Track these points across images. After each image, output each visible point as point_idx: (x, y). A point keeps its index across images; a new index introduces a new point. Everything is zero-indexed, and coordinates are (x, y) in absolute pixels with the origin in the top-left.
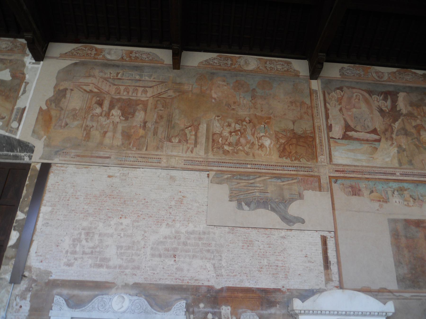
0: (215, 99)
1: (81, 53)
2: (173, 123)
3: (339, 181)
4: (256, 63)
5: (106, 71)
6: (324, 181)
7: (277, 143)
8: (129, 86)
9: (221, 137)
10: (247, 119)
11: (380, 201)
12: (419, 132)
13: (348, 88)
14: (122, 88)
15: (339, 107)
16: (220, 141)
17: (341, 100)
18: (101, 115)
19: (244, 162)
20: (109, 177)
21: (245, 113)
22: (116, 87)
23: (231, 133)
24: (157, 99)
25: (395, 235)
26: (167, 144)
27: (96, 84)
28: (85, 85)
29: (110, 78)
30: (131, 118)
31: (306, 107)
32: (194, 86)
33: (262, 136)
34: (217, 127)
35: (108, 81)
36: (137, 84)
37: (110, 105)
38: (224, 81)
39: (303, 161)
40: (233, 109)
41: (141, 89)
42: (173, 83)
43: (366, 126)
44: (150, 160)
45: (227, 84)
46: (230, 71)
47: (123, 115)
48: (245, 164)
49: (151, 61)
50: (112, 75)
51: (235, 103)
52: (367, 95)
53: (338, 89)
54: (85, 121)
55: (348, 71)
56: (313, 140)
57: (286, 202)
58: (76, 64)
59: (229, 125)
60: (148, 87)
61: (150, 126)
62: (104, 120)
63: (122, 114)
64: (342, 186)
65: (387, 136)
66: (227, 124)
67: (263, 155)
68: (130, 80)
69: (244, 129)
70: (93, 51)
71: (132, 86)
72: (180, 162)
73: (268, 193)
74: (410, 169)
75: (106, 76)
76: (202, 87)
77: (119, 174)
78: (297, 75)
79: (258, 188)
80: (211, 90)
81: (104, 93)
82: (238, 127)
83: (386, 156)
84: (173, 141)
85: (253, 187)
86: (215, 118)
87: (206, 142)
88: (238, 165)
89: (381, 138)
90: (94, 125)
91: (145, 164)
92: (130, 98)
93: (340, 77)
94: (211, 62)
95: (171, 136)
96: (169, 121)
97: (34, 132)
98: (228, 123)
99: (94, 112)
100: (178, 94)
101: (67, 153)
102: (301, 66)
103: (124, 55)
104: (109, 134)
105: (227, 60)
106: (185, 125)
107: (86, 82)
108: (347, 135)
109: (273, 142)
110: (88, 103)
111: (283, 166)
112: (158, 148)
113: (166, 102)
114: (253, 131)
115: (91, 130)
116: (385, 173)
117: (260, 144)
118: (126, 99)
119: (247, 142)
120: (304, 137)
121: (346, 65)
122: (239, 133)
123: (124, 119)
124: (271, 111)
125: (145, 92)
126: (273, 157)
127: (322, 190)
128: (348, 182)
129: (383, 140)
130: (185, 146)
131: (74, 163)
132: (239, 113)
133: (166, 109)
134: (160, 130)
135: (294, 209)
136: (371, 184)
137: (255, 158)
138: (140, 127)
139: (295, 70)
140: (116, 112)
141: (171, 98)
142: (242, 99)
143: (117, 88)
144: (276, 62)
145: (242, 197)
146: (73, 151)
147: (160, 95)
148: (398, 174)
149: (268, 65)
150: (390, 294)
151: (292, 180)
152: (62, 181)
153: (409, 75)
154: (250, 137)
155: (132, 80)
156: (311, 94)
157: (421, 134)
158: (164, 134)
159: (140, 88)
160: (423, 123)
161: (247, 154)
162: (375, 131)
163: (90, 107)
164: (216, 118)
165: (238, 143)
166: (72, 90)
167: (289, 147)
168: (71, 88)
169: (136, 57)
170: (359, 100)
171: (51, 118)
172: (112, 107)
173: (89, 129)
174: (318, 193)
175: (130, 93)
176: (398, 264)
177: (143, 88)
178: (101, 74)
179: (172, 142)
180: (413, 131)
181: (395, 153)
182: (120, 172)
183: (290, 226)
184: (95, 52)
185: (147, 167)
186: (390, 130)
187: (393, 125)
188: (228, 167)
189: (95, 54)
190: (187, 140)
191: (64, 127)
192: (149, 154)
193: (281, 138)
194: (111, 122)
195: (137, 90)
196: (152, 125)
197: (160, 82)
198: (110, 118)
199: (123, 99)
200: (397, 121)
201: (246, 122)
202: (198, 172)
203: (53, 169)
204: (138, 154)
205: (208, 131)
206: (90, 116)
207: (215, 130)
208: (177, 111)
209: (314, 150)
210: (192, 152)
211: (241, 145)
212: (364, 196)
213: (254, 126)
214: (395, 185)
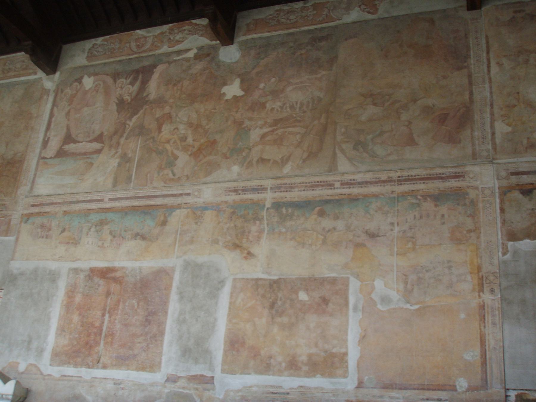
11: (68, 243)
55: (100, 49)
89: (103, 147)
121: (100, 40)
128: (39, 220)
129: (106, 149)
148: (106, 199)
157: (162, 130)
162: (99, 139)
170: (97, 92)
187: (128, 122)
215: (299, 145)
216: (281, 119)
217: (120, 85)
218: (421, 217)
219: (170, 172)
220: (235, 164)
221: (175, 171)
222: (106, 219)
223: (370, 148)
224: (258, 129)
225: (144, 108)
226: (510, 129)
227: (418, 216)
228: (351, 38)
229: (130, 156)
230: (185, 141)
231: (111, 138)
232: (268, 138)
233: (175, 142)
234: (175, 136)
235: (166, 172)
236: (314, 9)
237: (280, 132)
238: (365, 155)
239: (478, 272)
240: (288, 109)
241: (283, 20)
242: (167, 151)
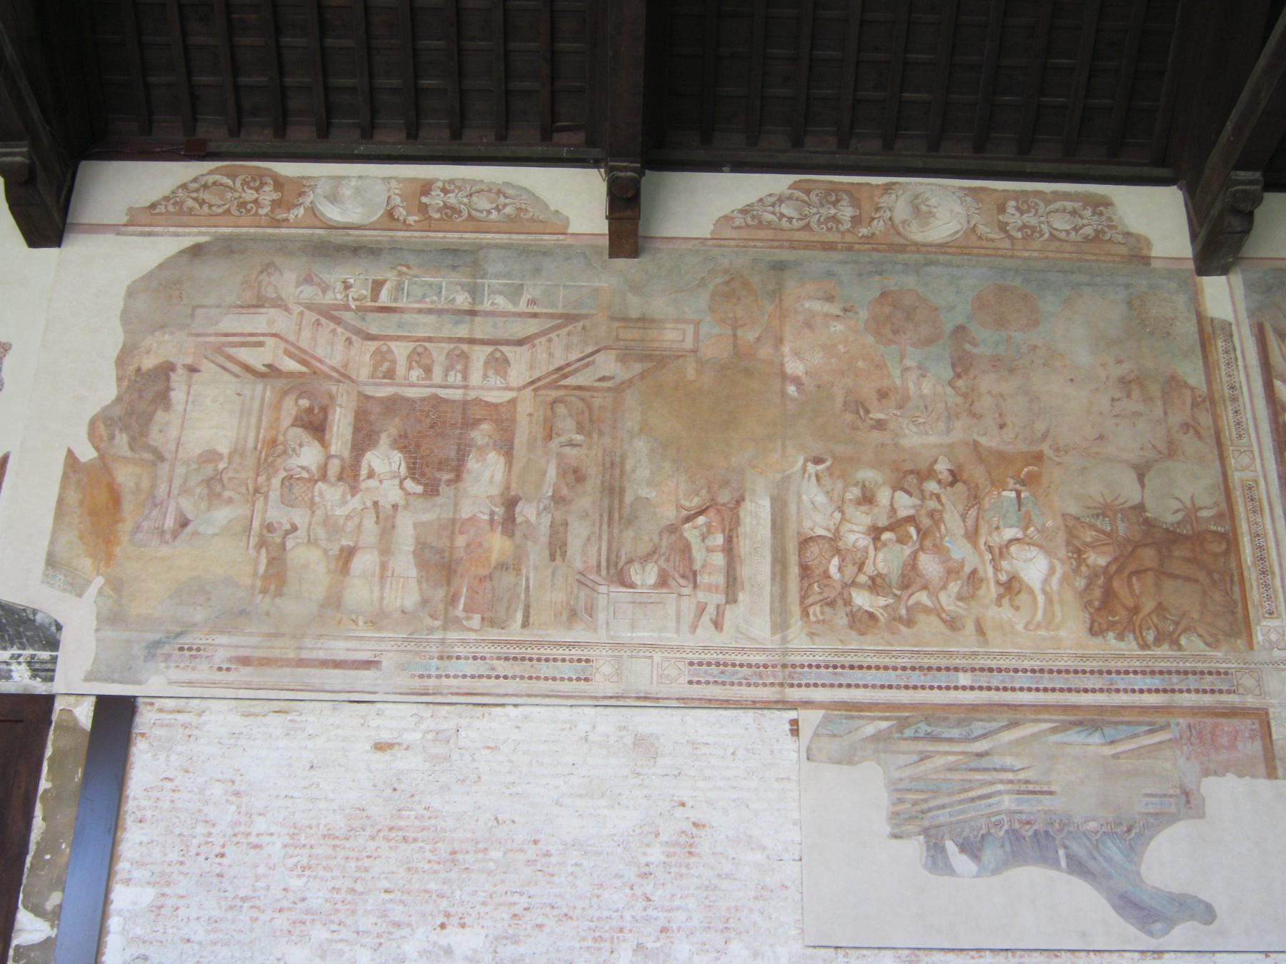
0: (796, 381)
1: (215, 200)
2: (628, 499)
4: (959, 209)
5: (325, 277)
7: (1076, 571)
8: (430, 340)
9: (838, 551)
10: (942, 467)
14: (401, 350)
16: (833, 570)
18: (324, 477)
19: (943, 662)
20: (380, 747)
21: (932, 439)
22: (372, 346)
23: (876, 532)
24: (554, 394)
26: (609, 593)
27: (292, 338)
28: (243, 344)
29: (347, 308)
30: (449, 483)
31: (1189, 401)
32: (704, 329)
33: (1011, 542)
34: (815, 508)
35: (338, 321)
36: (462, 331)
37: (357, 430)
38: (830, 299)
39: (1191, 643)
40: (880, 425)
41: (480, 355)
42: (613, 319)
44: (545, 669)
45: (845, 310)
46: (850, 249)
47: (415, 471)
48: (948, 669)
49: (514, 223)
50: (352, 293)
51: (883, 395)
54: (259, 504)
56: (1227, 552)
57: (1129, 831)
58: (196, 251)
59: (867, 499)
60: (508, 343)
61: (533, 519)
62: (338, 496)
63: (409, 468)
66: (855, 492)
67: (1020, 627)
68: (430, 311)
69: (931, 514)
70: (266, 188)
71: (442, 340)
72: (673, 672)
73: (1051, 793)
75: (329, 299)
76: (740, 333)
77: (418, 736)
78: (1138, 255)
79: (1010, 776)
80: (780, 340)
81: (327, 377)
82: (905, 504)
84: (637, 579)
85: (986, 770)
86: (804, 470)
87: (773, 579)
88: (917, 678)
90: (297, 521)
91: (524, 686)
92: (436, 397)
94: (769, 217)
95: (623, 559)
96: (613, 490)
97: (51, 561)
98: (864, 486)
99: (294, 462)
100: (637, 368)
101: (195, 652)
102: (1155, 216)
103: (397, 200)
104: (365, 561)
105: (835, 204)
106: (679, 507)
107: (249, 329)
109: (1057, 563)
110: (264, 424)
111: (1109, 672)
112: (573, 614)
113: (589, 406)
114: (970, 522)
115: (289, 545)
117: (1003, 578)
118: (423, 400)
119: (949, 572)
120: (1187, 538)
122: (912, 530)
123: (420, 489)
124: (1040, 426)
125: (499, 364)
130: (685, 603)
131: (231, 693)
132: (905, 442)
133: (595, 436)
134: (578, 533)
135: (1167, 862)
137: (986, 643)
138: (492, 521)
139: (1128, 234)
140: (385, 461)
141: (609, 389)
142: (912, 377)
143: (377, 352)
144: (1048, 203)
145: (943, 817)
146: (222, 639)
147: (565, 376)
149: (1013, 217)
151: (1151, 732)
152: (187, 771)
154: (960, 550)
155: (440, 312)
156: (1205, 343)
158: (593, 550)
159: (477, 348)
161: (953, 624)
163: (274, 442)
164: (811, 468)
165: (910, 577)
166: (193, 369)
167: (1130, 585)
168: (189, 361)
169: (446, 206)
171: (115, 499)
172: (364, 439)
173: (279, 540)
175: (438, 372)
177: (490, 349)
178: (308, 292)
179: (632, 586)
182: (423, 727)
183: (1150, 934)
184: (276, 196)
185: (533, 700)
188: (874, 686)
189: (276, 204)
190: (695, 573)
191: (175, 535)
192: (540, 644)
194: (369, 504)
195: (464, 356)
196: (539, 514)
197: (561, 316)
198: (363, 486)
199: (408, 399)
201: (939, 482)
202: (751, 712)
203: (145, 719)
204: (493, 642)
205: (778, 525)
206: (276, 482)
207: (807, 524)
208: (641, 446)
209: (1237, 594)
210: (717, 624)
211: (925, 588)
213: (975, 498)
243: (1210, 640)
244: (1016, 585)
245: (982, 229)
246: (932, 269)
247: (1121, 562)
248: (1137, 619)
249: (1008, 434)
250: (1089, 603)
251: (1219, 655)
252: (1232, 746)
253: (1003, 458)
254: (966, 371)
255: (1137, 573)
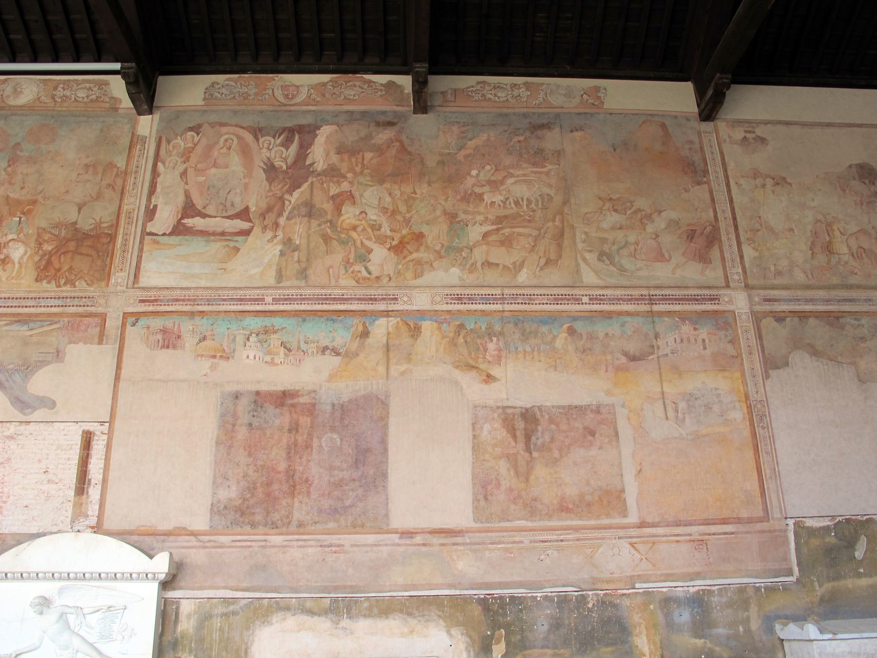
3: (143, 322)
4: (35, 90)
6: (113, 323)
7: (37, 253)
11: (214, 357)
12: (338, 210)
13: (212, 125)
15: (181, 168)
17: (191, 152)
25: (228, 426)
31: (115, 173)
39: (81, 284)
43: (228, 204)
52: (249, 137)
53: (191, 129)
55: (224, 91)
56: (109, 242)
64: (145, 330)
65: (266, 223)
67: (4, 279)
74: (299, 288)
83: (257, 262)
89: (252, 228)
93: (202, 103)
108: (184, 225)
109: (29, 250)
116: (241, 300)
120: (93, 236)
121: (221, 78)
124: (41, 188)
126: (23, 281)
127: (105, 341)
128: (157, 323)
129: (257, 231)
135: (40, 383)
136: (203, 324)
139: (112, 98)
144: (78, 84)
148: (269, 299)
150: (192, 538)
153: (355, 86)
157: (343, 211)
160: (354, 190)
162: (244, 214)
170: (229, 149)
174: (95, 348)
176: (220, 479)
180: (328, 206)
181: (274, 255)
183: (24, 414)
186: (276, 209)
187: (287, 196)
193: (47, 241)
200: (300, 188)
209: (108, 262)
212: (184, 349)
214: (255, 323)
215: (533, 249)
216: (506, 217)
217: (265, 145)
218: (682, 341)
219: (363, 269)
220: (454, 266)
221: (371, 268)
222: (273, 326)
223: (617, 260)
224: (477, 224)
225: (310, 180)
226: (756, 254)
227: (678, 340)
228: (577, 130)
229: (297, 242)
230: (379, 229)
231: (263, 216)
232: (490, 239)
233: (364, 230)
234: (363, 222)
235: (356, 268)
236: (527, 90)
237: (507, 231)
238: (612, 268)
239: (746, 400)
240: (513, 205)
241: (489, 96)
242: (354, 241)
243: (89, 282)
244: (7, 260)
245: (43, 98)
246: (13, 117)
247: (58, 248)
248: (58, 274)
249: (24, 192)
250: (39, 267)
251: (92, 289)
252: (86, 330)
253: (18, 202)
254: (14, 164)
255: (64, 253)
